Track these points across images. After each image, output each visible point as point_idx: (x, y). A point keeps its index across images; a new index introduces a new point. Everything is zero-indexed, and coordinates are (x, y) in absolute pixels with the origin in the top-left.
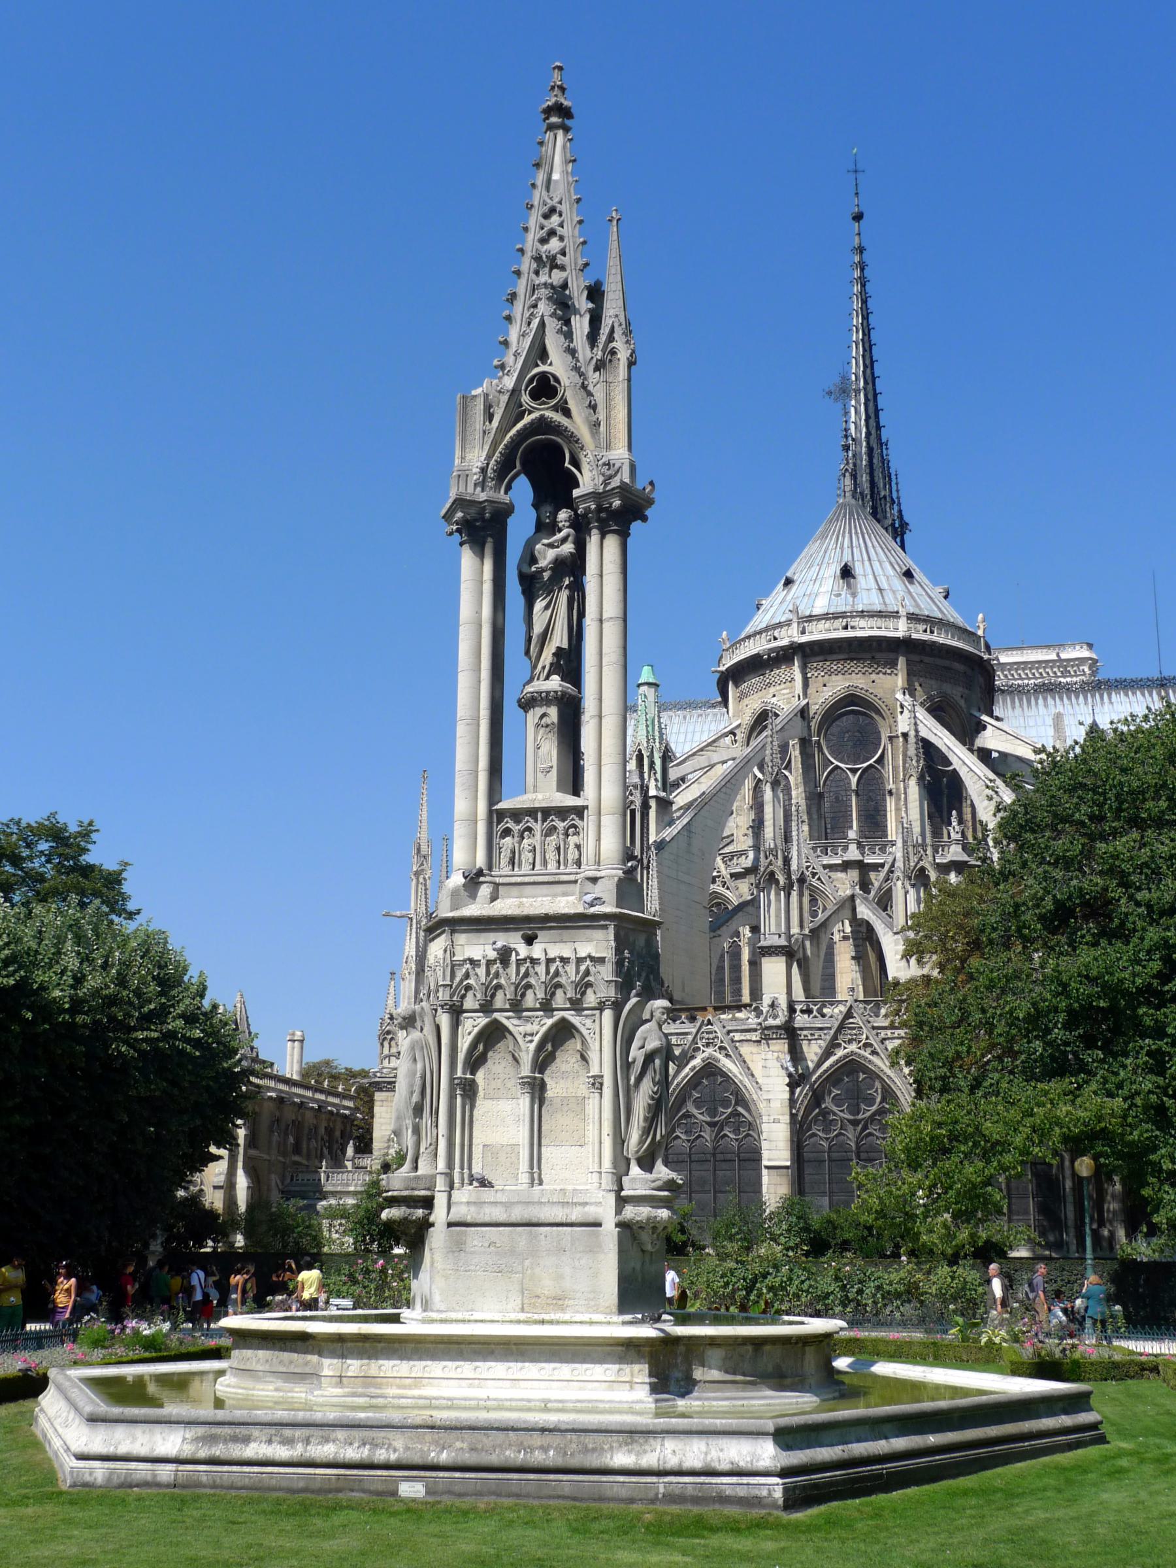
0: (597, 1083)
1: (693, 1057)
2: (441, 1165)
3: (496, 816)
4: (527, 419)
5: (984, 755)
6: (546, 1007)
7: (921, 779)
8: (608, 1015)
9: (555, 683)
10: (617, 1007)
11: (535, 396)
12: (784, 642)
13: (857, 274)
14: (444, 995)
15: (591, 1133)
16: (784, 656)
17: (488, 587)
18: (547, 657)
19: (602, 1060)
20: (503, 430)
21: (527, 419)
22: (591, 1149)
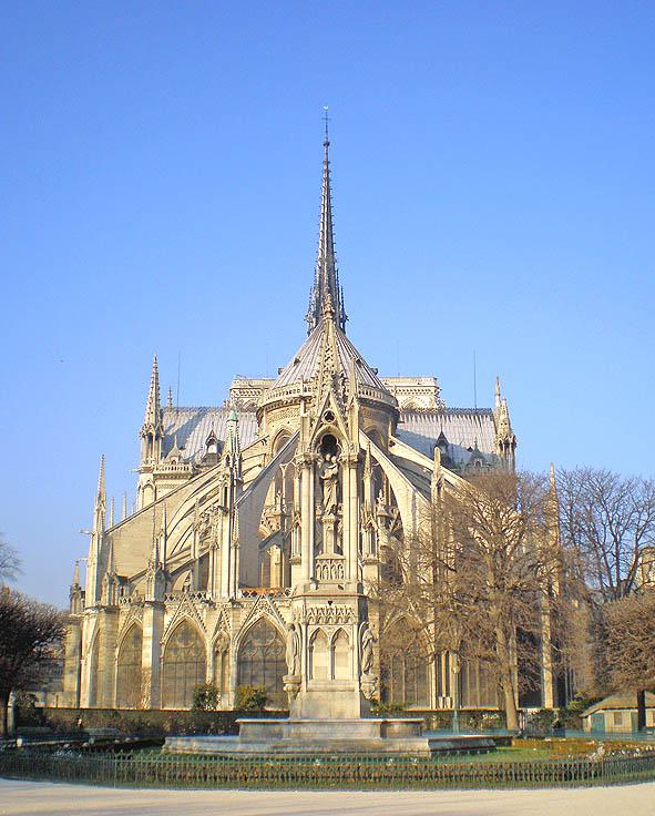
0: (353, 648)
1: (255, 613)
2: (303, 672)
3: (315, 561)
4: (324, 427)
5: (392, 458)
6: (337, 622)
7: (372, 479)
8: (356, 627)
9: (332, 517)
10: (359, 626)
11: (326, 419)
12: (296, 395)
13: (325, 176)
14: (302, 620)
15: (350, 662)
16: (295, 402)
17: (312, 484)
18: (329, 507)
19: (354, 640)
20: (316, 431)
21: (324, 427)
22: (349, 670)
